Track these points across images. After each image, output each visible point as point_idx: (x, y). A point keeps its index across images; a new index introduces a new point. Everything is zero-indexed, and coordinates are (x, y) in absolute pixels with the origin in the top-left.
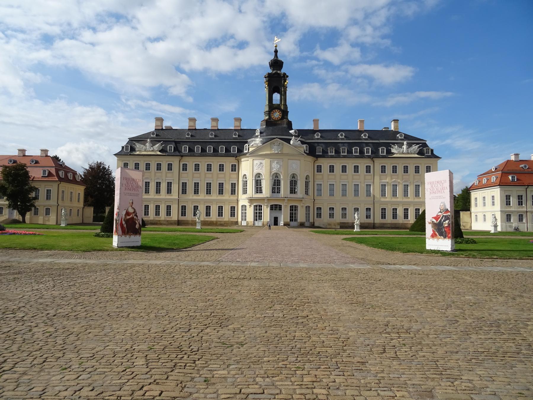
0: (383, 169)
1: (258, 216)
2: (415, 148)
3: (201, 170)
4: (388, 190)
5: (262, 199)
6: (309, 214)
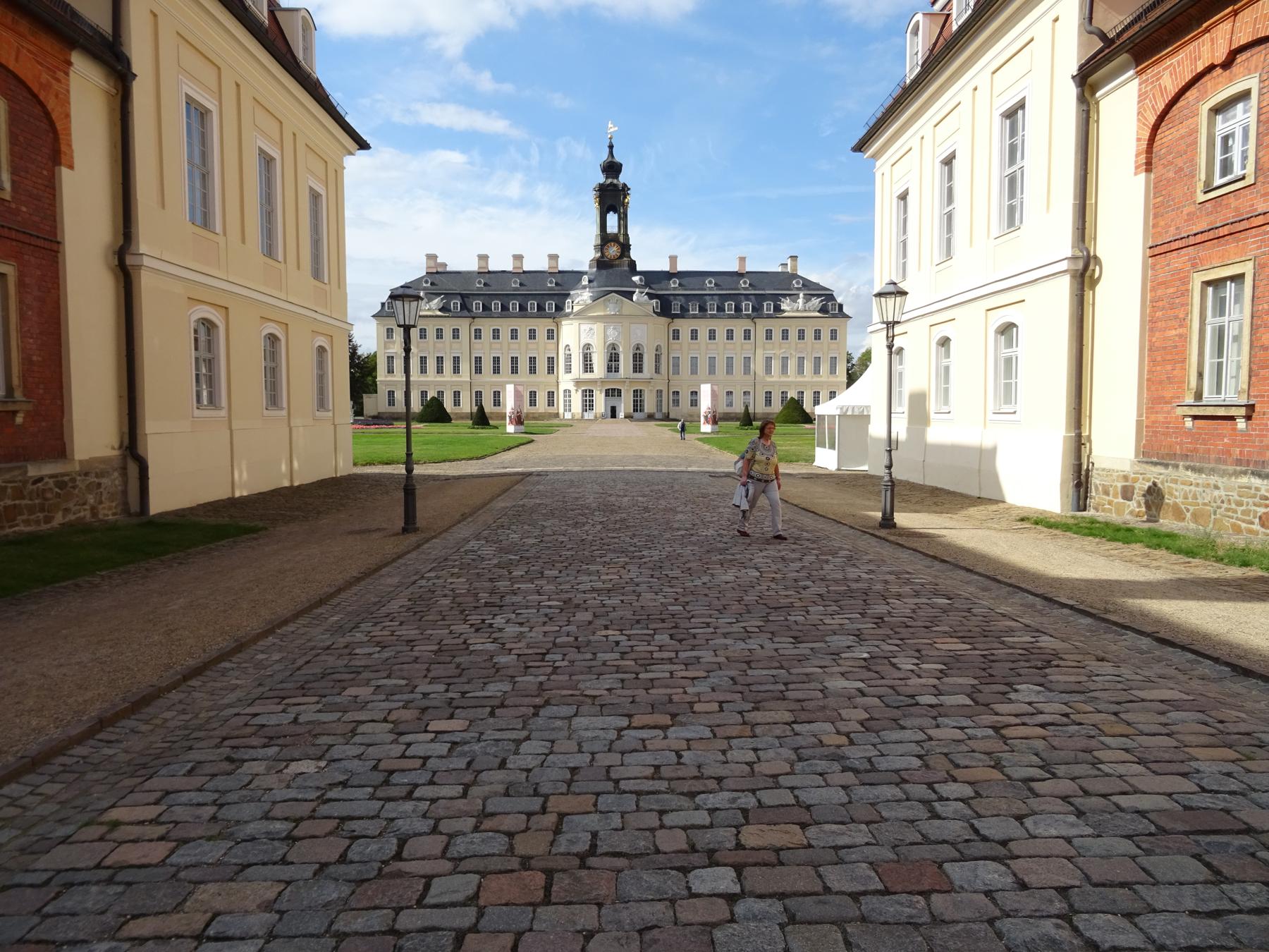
0: (769, 335)
1: (588, 405)
2: (816, 302)
3: (503, 338)
4: (776, 365)
5: (594, 382)
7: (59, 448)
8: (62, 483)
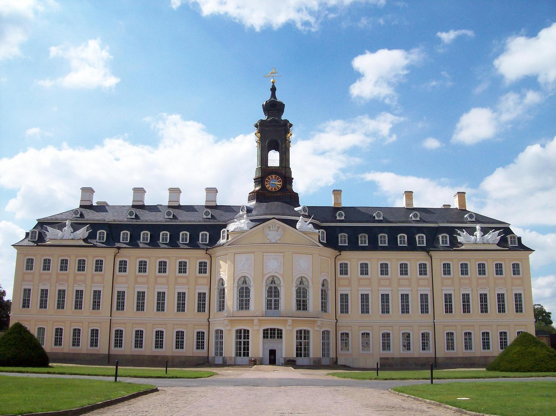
0: (447, 269)
6: (328, 344)
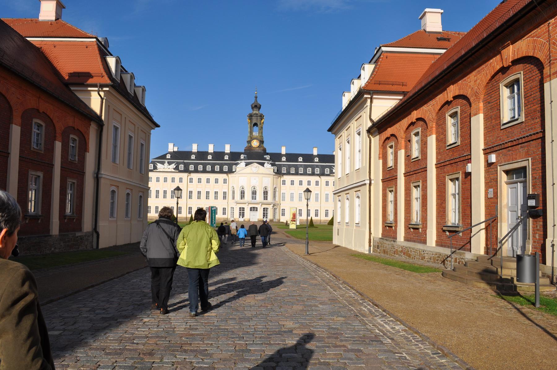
7: (80, 229)
8: (81, 238)
